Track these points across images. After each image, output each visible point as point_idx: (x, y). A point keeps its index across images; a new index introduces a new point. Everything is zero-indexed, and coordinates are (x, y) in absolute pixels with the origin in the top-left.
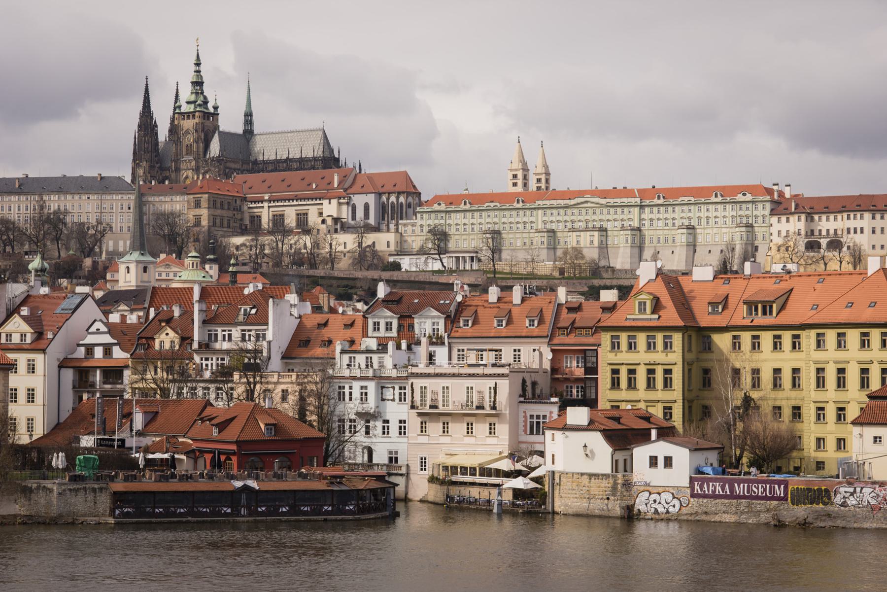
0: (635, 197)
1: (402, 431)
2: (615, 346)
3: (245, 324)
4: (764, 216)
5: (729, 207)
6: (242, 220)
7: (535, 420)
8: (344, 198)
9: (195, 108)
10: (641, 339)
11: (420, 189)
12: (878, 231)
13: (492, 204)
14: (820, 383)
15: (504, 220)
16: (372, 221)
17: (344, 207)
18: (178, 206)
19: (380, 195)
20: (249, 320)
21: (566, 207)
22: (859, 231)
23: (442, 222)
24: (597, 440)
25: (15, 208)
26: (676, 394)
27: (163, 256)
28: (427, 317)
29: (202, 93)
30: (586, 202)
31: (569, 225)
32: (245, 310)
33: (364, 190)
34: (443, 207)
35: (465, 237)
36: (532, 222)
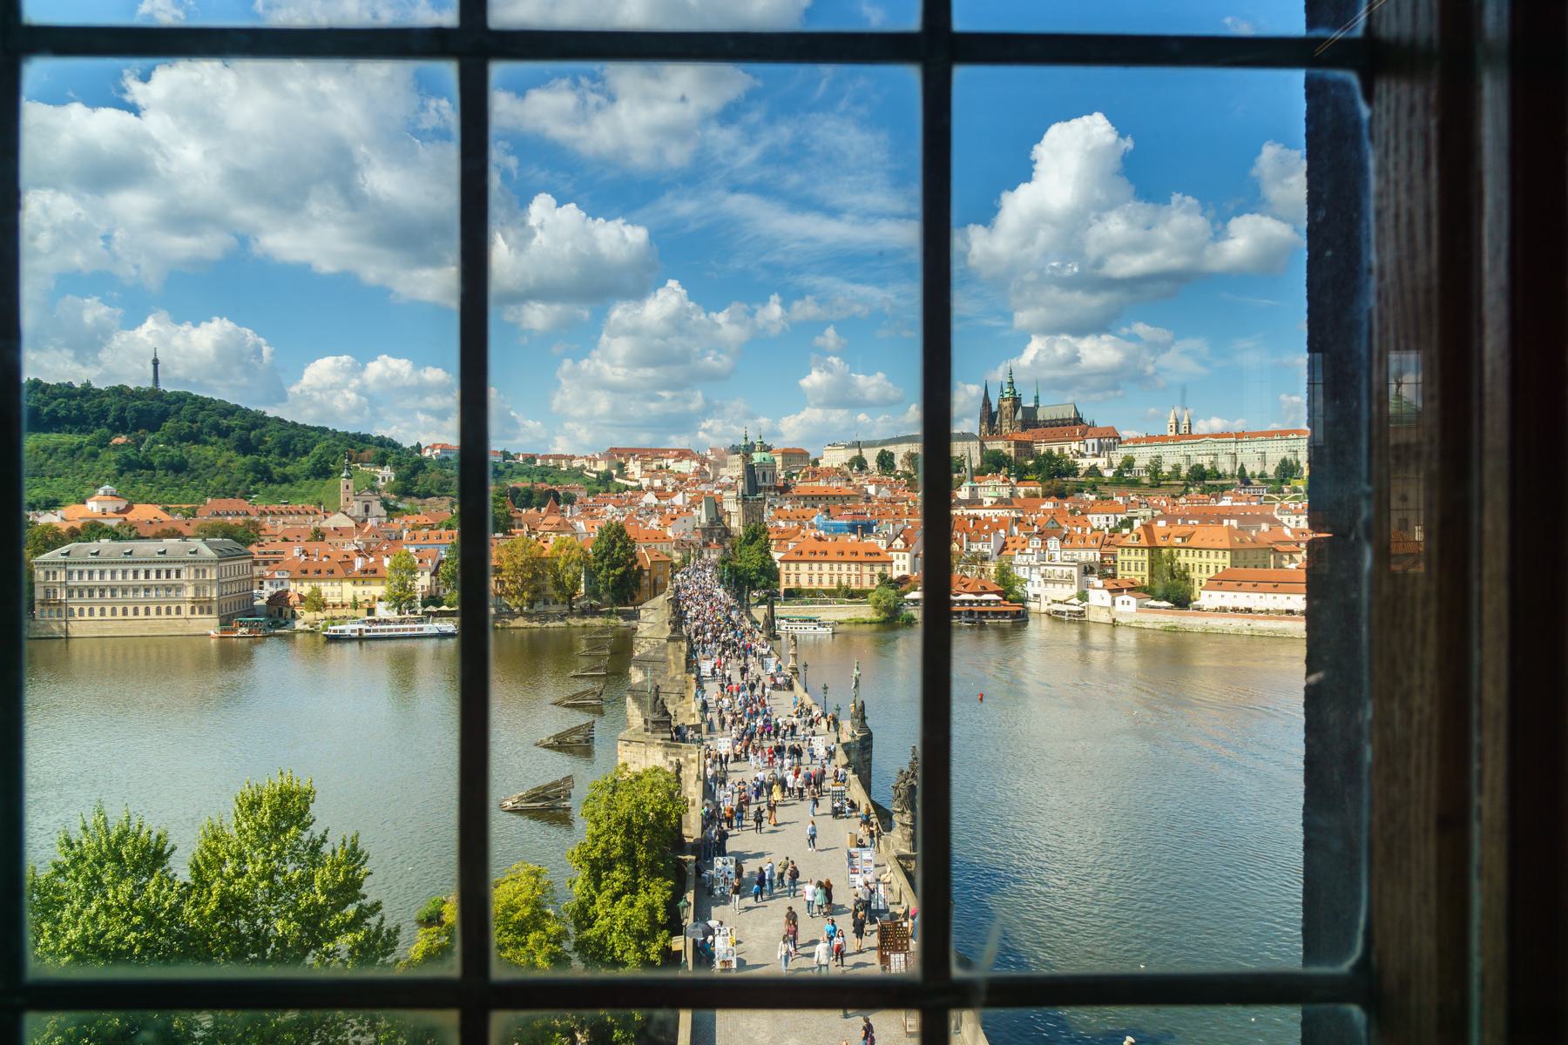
1: (1039, 585)
14: (1200, 570)
16: (1096, 452)
24: (1106, 593)
26: (1146, 573)
34: (1132, 444)
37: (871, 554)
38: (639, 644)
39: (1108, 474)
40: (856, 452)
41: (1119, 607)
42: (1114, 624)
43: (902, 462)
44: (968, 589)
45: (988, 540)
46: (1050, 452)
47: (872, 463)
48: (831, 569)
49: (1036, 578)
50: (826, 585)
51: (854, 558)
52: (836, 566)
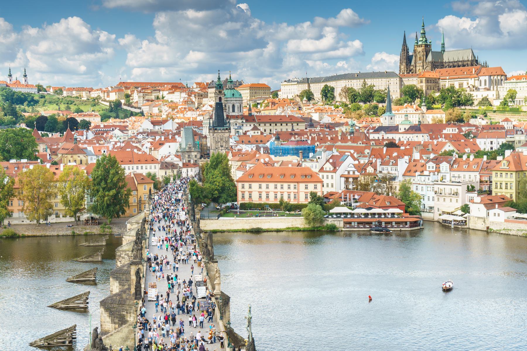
1: (433, 200)
2: (496, 176)
3: (392, 165)
6: (438, 86)
7: (470, 198)
10: (504, 173)
11: (506, 74)
16: (487, 86)
17: (477, 81)
20: (393, 164)
24: (482, 206)
25: (355, 84)
26: (513, 191)
29: (425, 37)
33: (484, 75)
34: (515, 81)
37: (306, 176)
38: (120, 256)
39: (496, 104)
40: (305, 87)
41: (492, 218)
42: (488, 232)
43: (340, 95)
44: (378, 204)
45: (396, 164)
46: (453, 87)
47: (318, 96)
48: (276, 188)
49: (432, 194)
50: (272, 200)
51: (292, 179)
52: (279, 185)
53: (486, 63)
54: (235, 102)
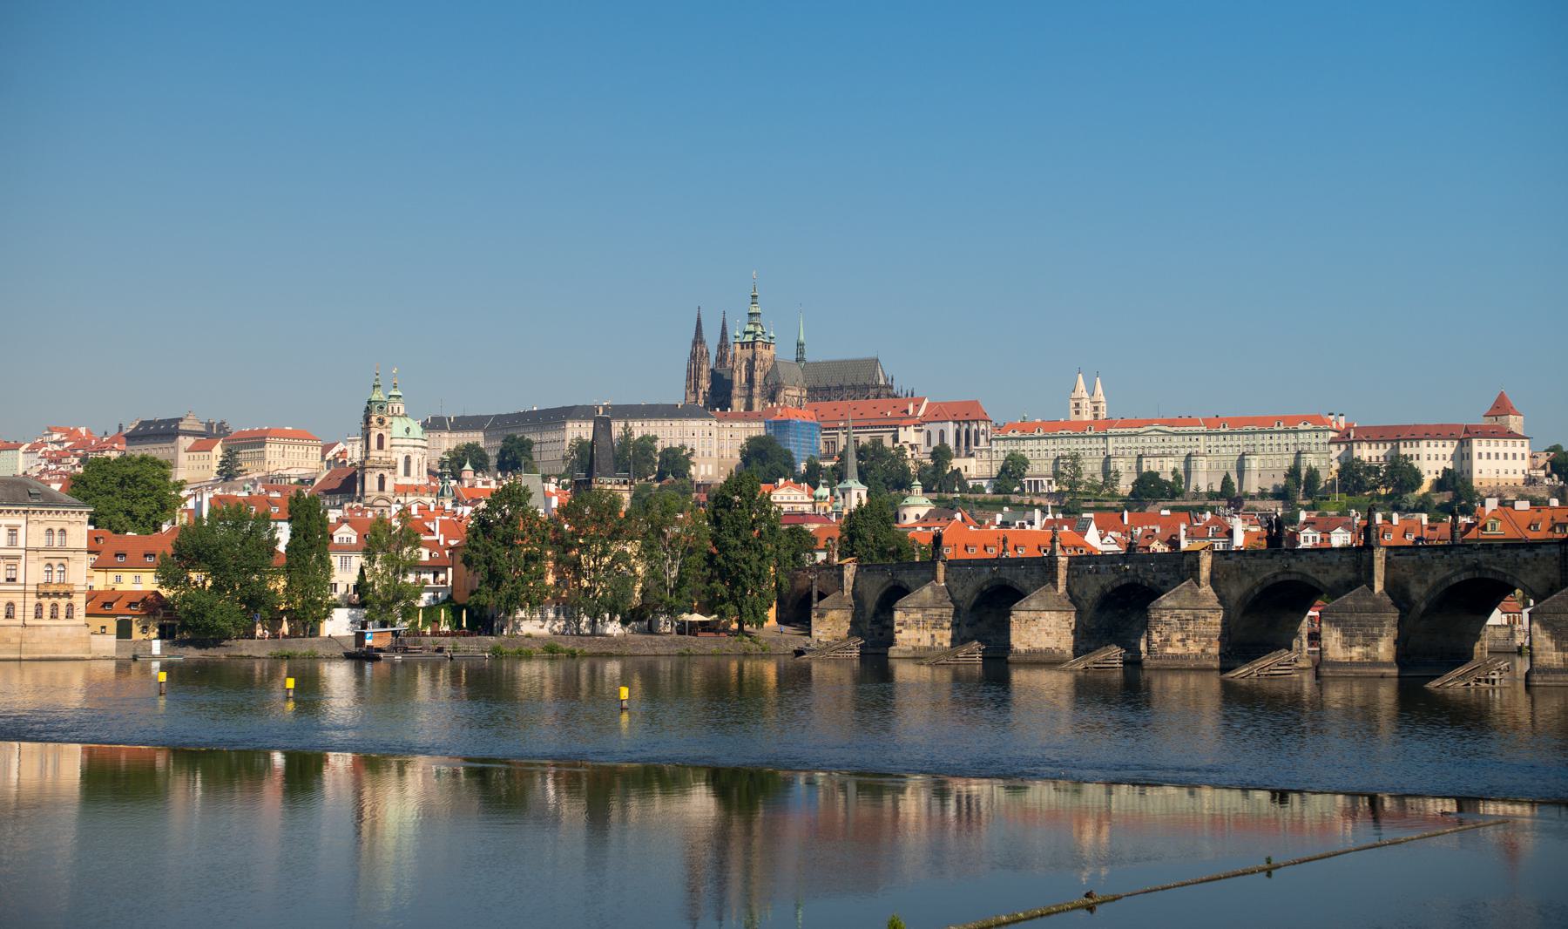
0: (1200, 426)
4: (1324, 443)
5: (1292, 436)
8: (919, 426)
9: (754, 338)
12: (1433, 457)
13: (1065, 432)
15: (1077, 446)
18: (754, 432)
19: (954, 422)
21: (1136, 434)
22: (1415, 457)
23: (1017, 448)
27: (782, 481)
28: (1339, 533)
30: (1156, 430)
31: (1140, 452)
32: (1213, 529)
34: (1017, 434)
35: (1040, 462)
36: (1103, 449)
38: (1159, 620)
53: (912, 395)
54: (412, 449)
